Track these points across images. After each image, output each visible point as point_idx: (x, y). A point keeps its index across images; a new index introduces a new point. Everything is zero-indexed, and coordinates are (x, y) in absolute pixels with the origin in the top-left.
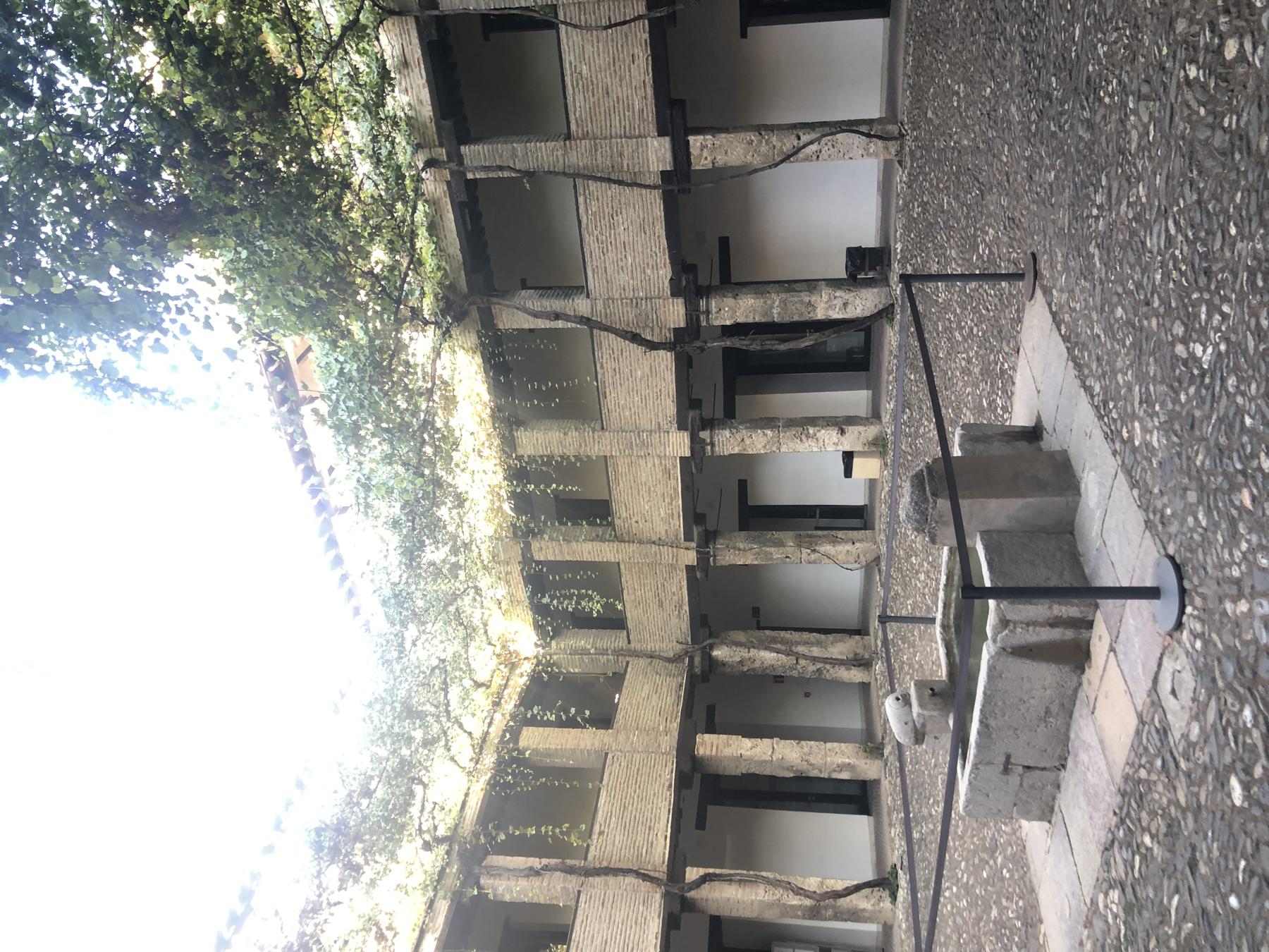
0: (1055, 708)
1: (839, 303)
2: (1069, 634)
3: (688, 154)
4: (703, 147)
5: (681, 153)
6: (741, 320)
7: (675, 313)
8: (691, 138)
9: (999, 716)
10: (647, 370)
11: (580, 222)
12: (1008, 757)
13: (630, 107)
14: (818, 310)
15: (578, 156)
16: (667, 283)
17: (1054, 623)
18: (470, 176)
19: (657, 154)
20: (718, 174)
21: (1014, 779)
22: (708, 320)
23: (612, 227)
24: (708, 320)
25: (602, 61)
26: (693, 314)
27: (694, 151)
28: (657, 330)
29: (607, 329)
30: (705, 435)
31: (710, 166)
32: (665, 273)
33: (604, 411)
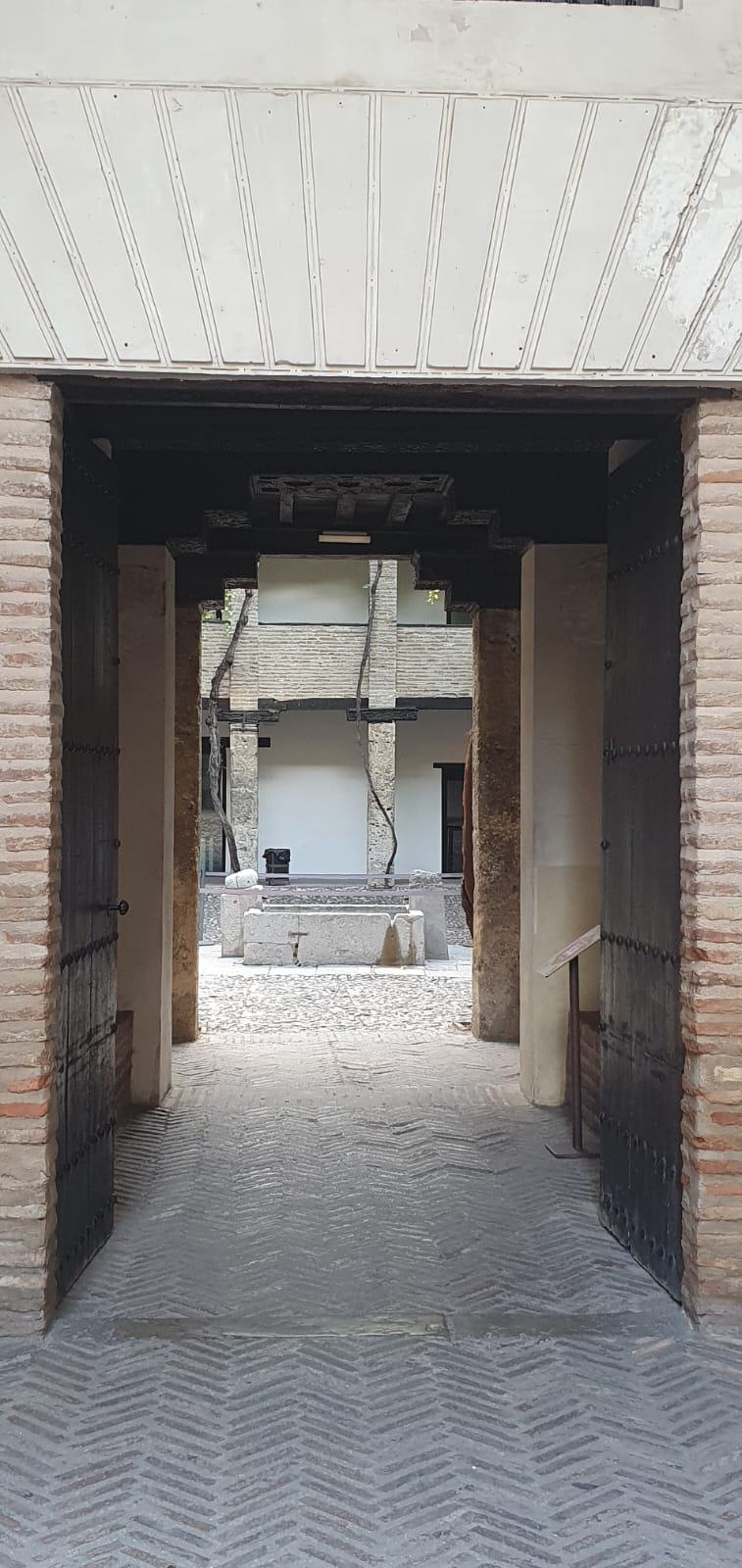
0: (347, 954)
1: (247, 844)
2: (404, 954)
5: (382, 716)
7: (243, 701)
8: (393, 724)
12: (306, 934)
13: (419, 678)
14: (241, 826)
15: (383, 630)
16: (271, 696)
17: (412, 947)
19: (382, 697)
20: (364, 743)
22: (237, 730)
24: (237, 730)
25: (455, 659)
26: (241, 717)
27: (383, 726)
28: (227, 683)
29: (235, 638)
31: (370, 739)
32: (281, 696)
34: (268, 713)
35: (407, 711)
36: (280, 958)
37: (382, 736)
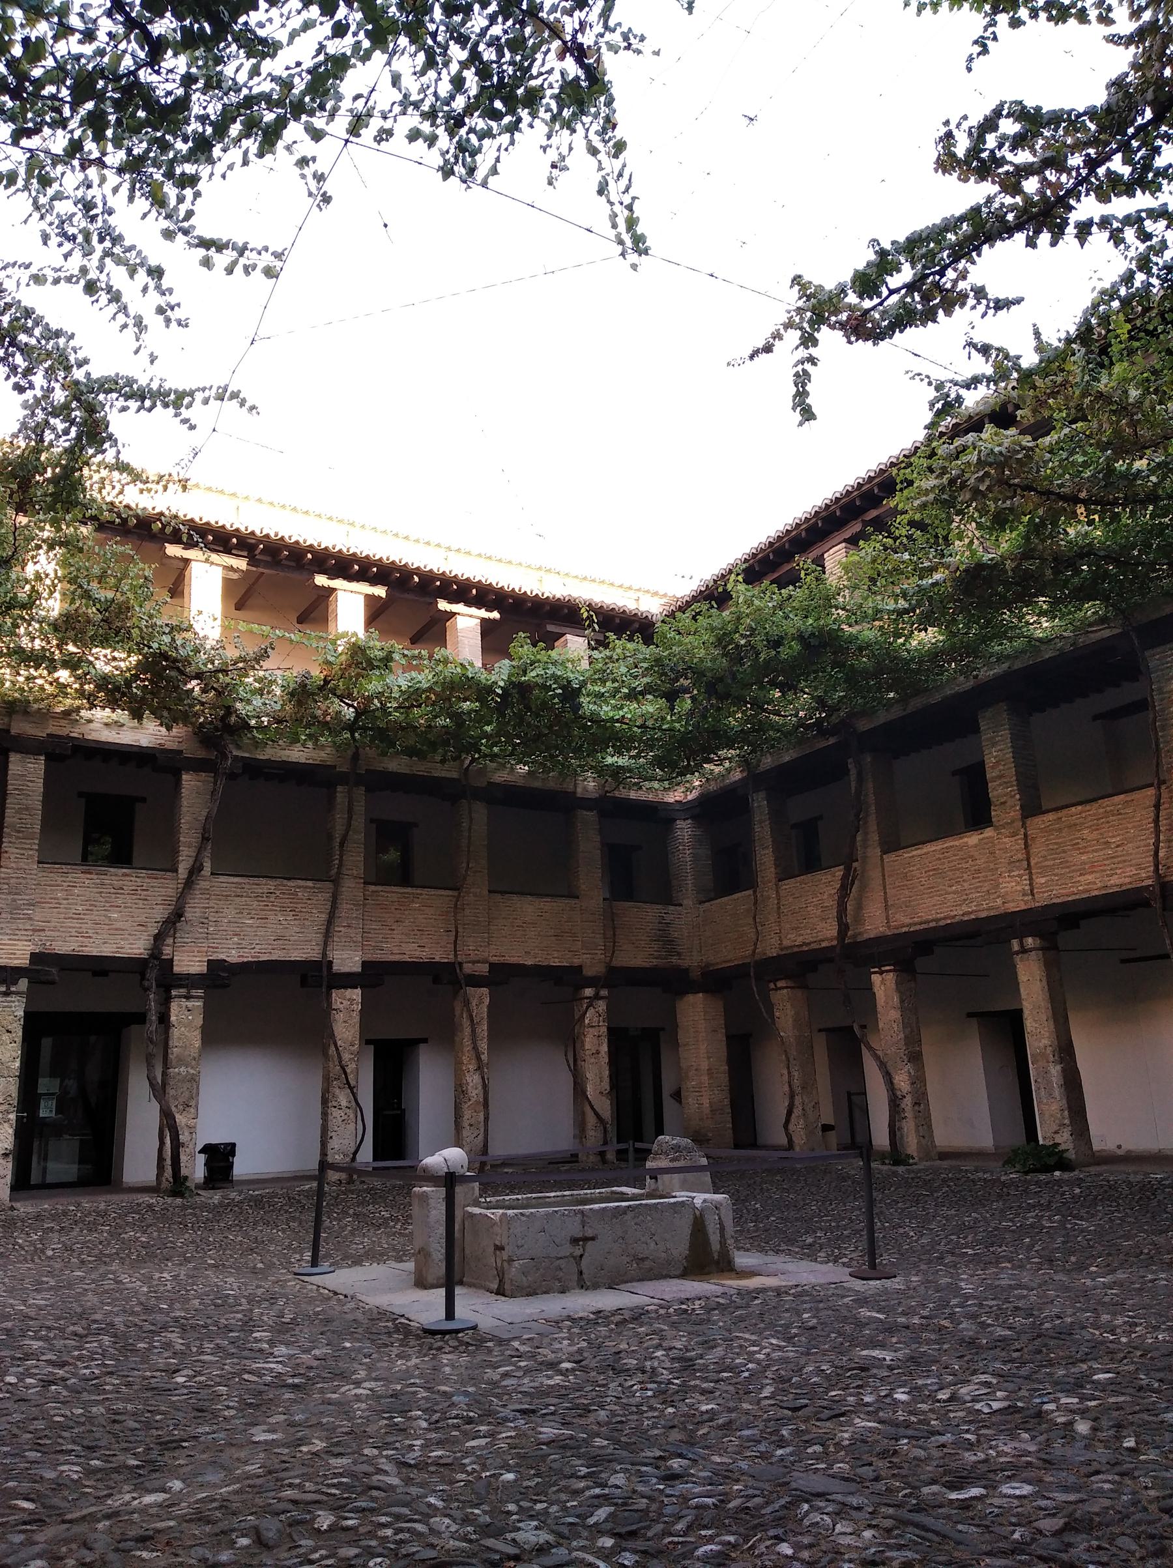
0: (647, 1264)
3: (346, 987)
4: (351, 1000)
5: (347, 981)
6: (175, 1033)
7: (189, 960)
8: (359, 991)
9: (636, 1220)
10: (118, 925)
11: (289, 879)
12: (593, 1239)
16: (222, 957)
18: (339, 788)
19: (347, 960)
21: (567, 1250)
23: (283, 909)
24: (180, 997)
26: (189, 981)
27: (349, 993)
30: (23, 984)
32: (232, 955)
33: (65, 868)
34: (219, 978)
35: (373, 976)
36: (560, 1280)
37: (347, 1004)
